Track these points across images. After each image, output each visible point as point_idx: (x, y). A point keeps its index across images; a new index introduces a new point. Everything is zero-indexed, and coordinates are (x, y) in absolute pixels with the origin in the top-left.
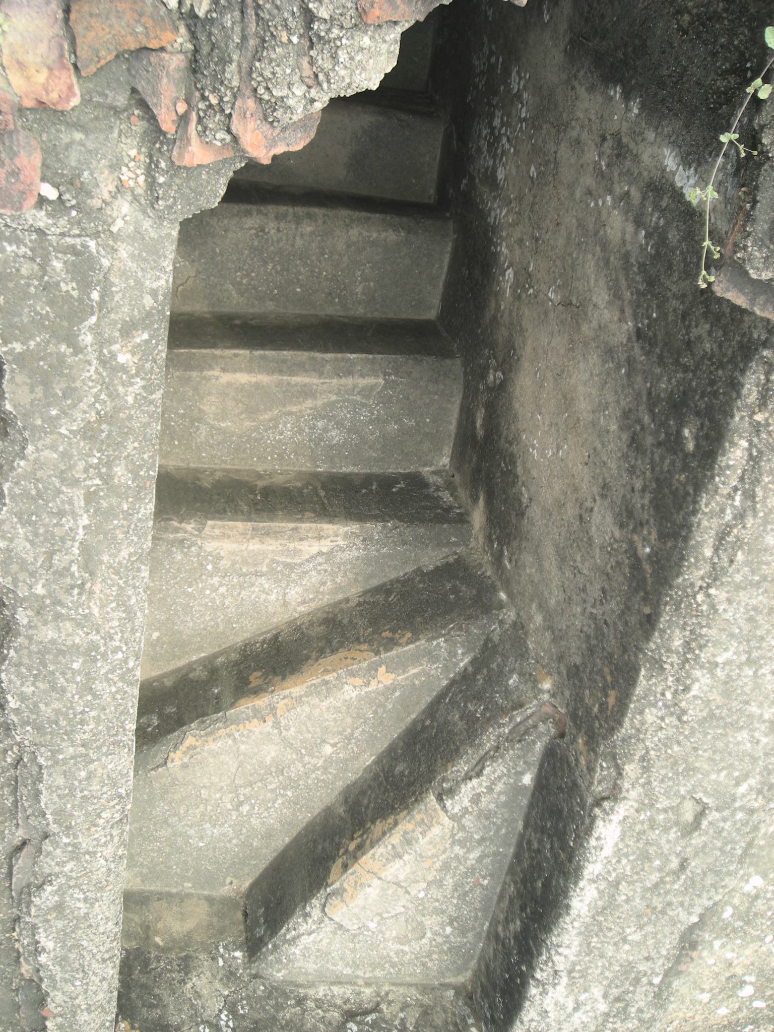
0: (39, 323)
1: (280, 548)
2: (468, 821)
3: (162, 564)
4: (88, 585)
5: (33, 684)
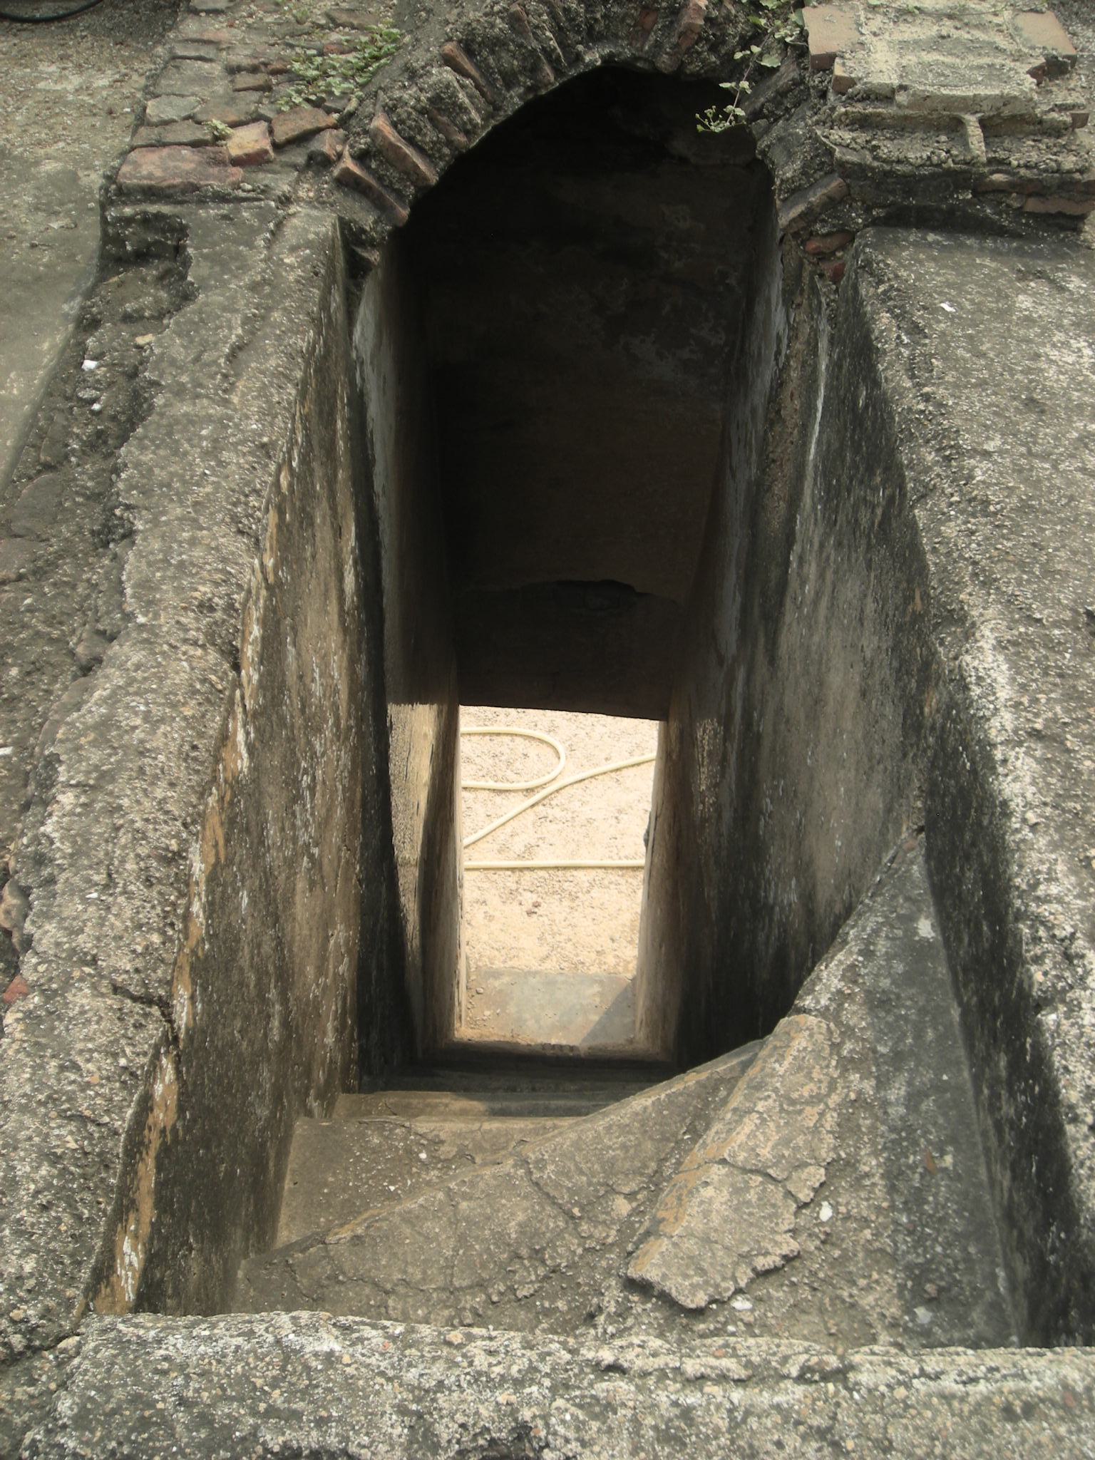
0: (226, 239)
1: (531, 1126)
2: (854, 1014)
3: (349, 1150)
4: (232, 379)
5: (154, 453)
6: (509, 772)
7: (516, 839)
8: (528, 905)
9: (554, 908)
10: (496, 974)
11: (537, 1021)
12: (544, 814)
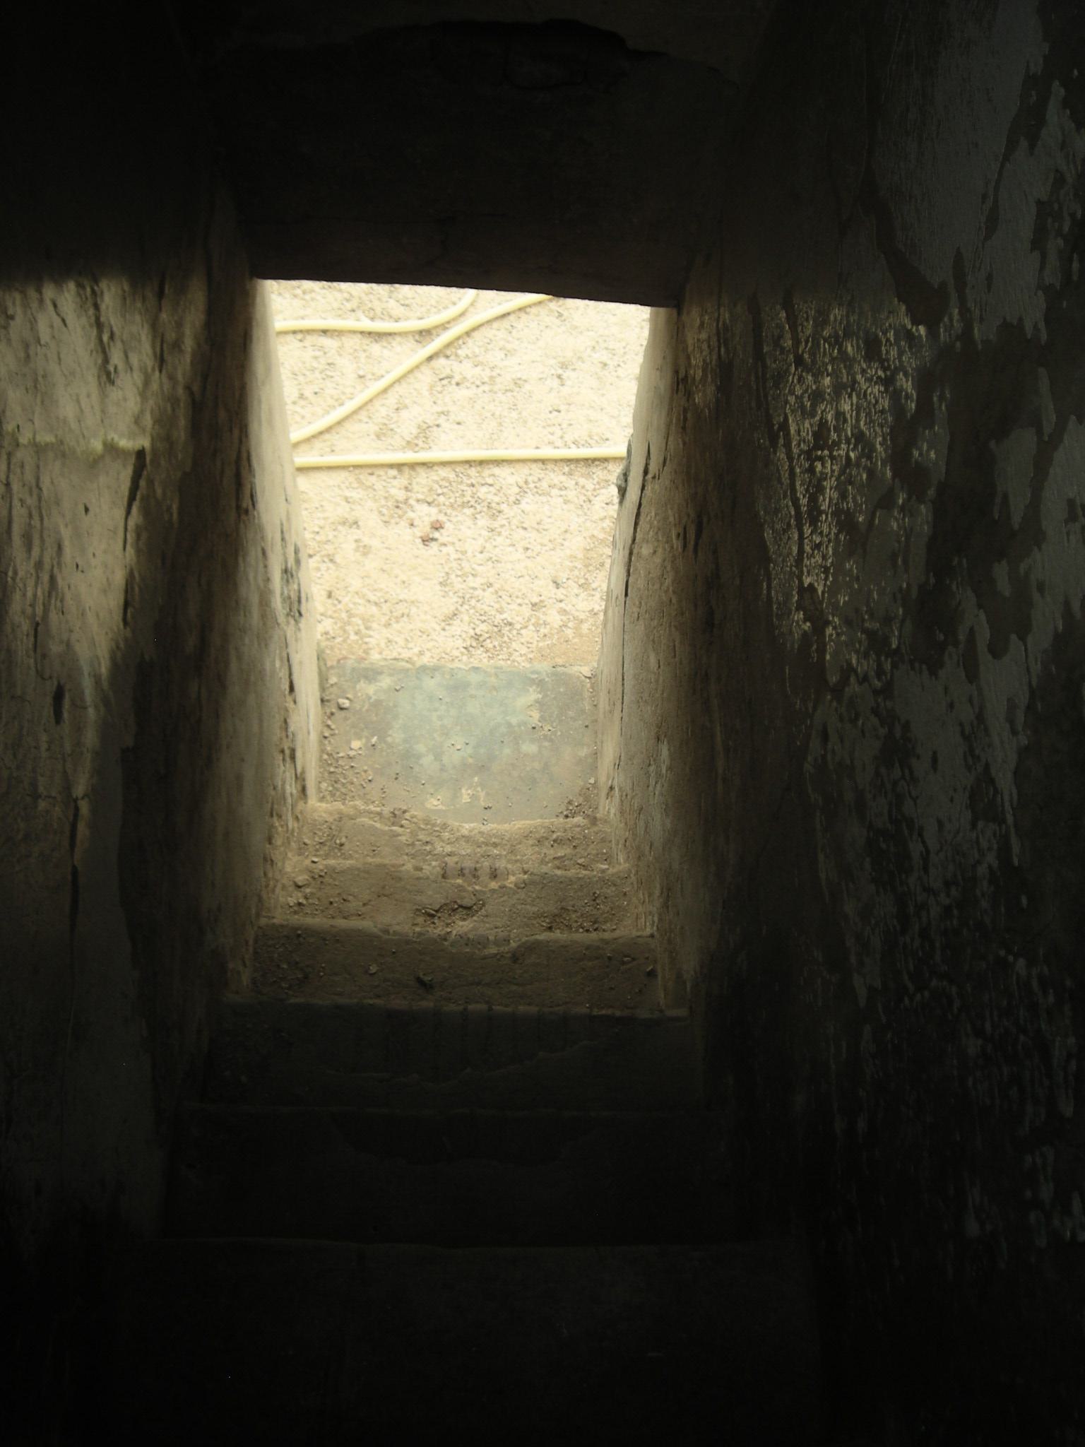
6: (392, 303)
7: (404, 413)
8: (423, 528)
9: (466, 531)
10: (371, 674)
11: (438, 757)
12: (447, 372)
